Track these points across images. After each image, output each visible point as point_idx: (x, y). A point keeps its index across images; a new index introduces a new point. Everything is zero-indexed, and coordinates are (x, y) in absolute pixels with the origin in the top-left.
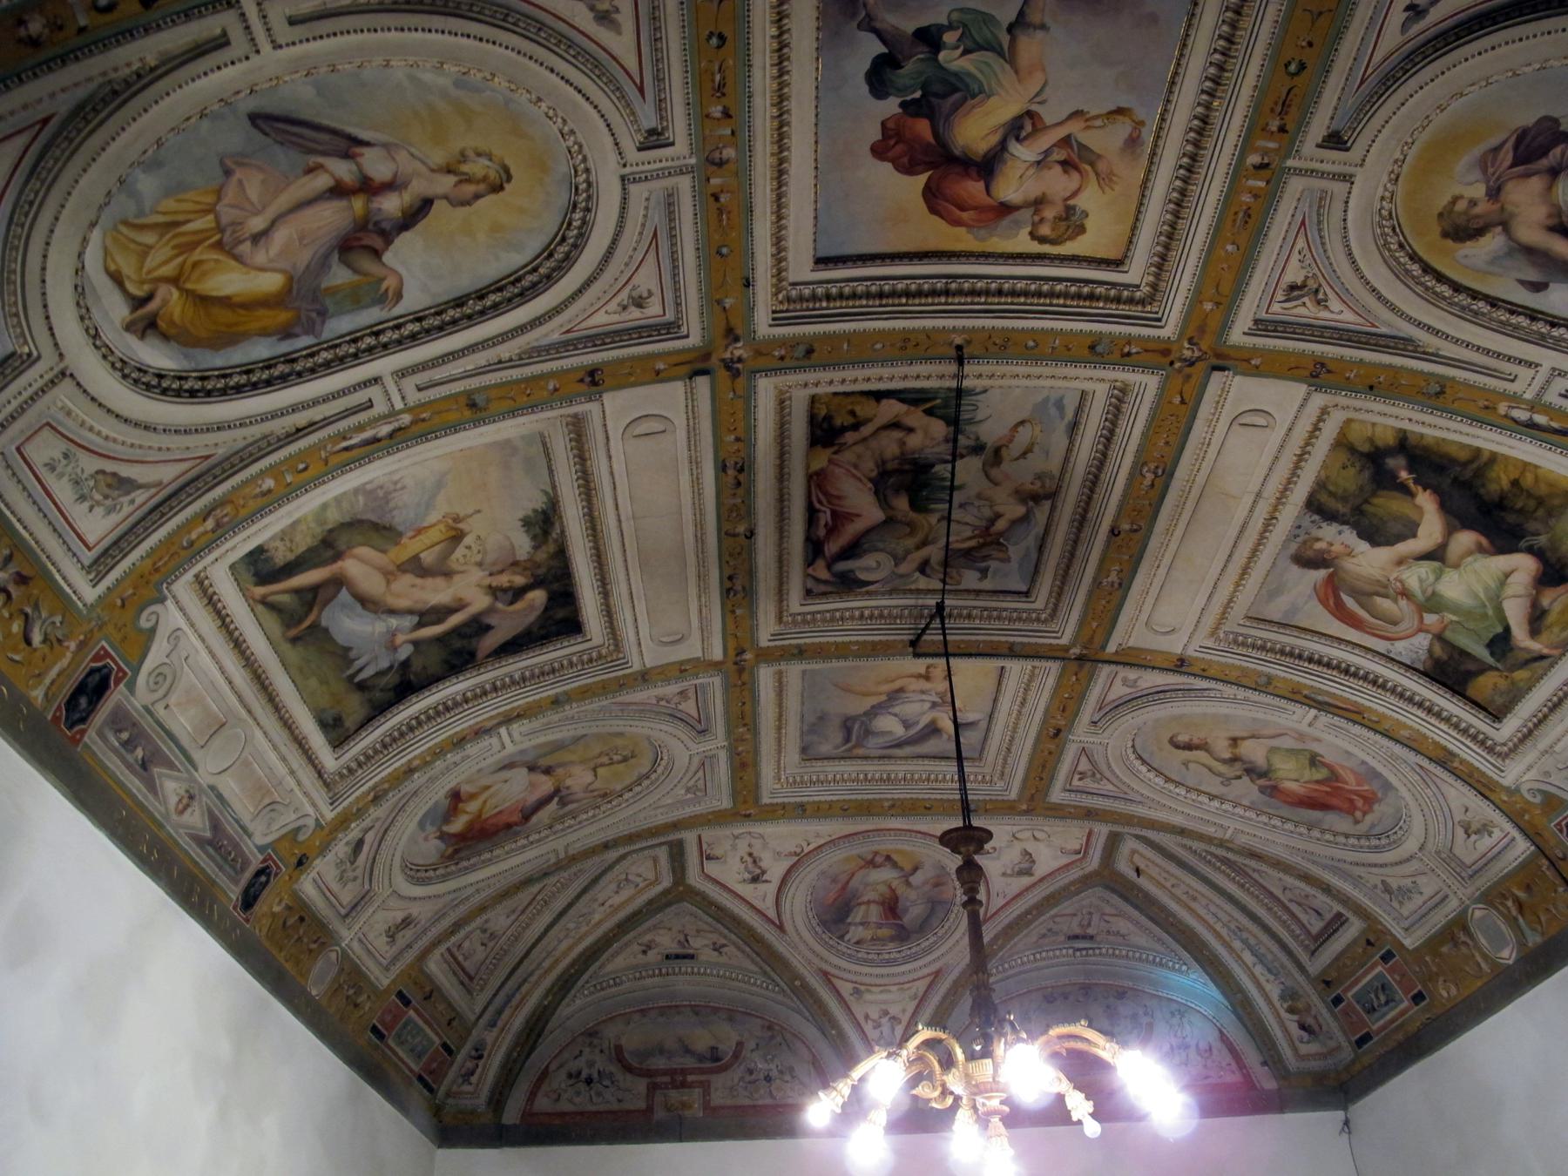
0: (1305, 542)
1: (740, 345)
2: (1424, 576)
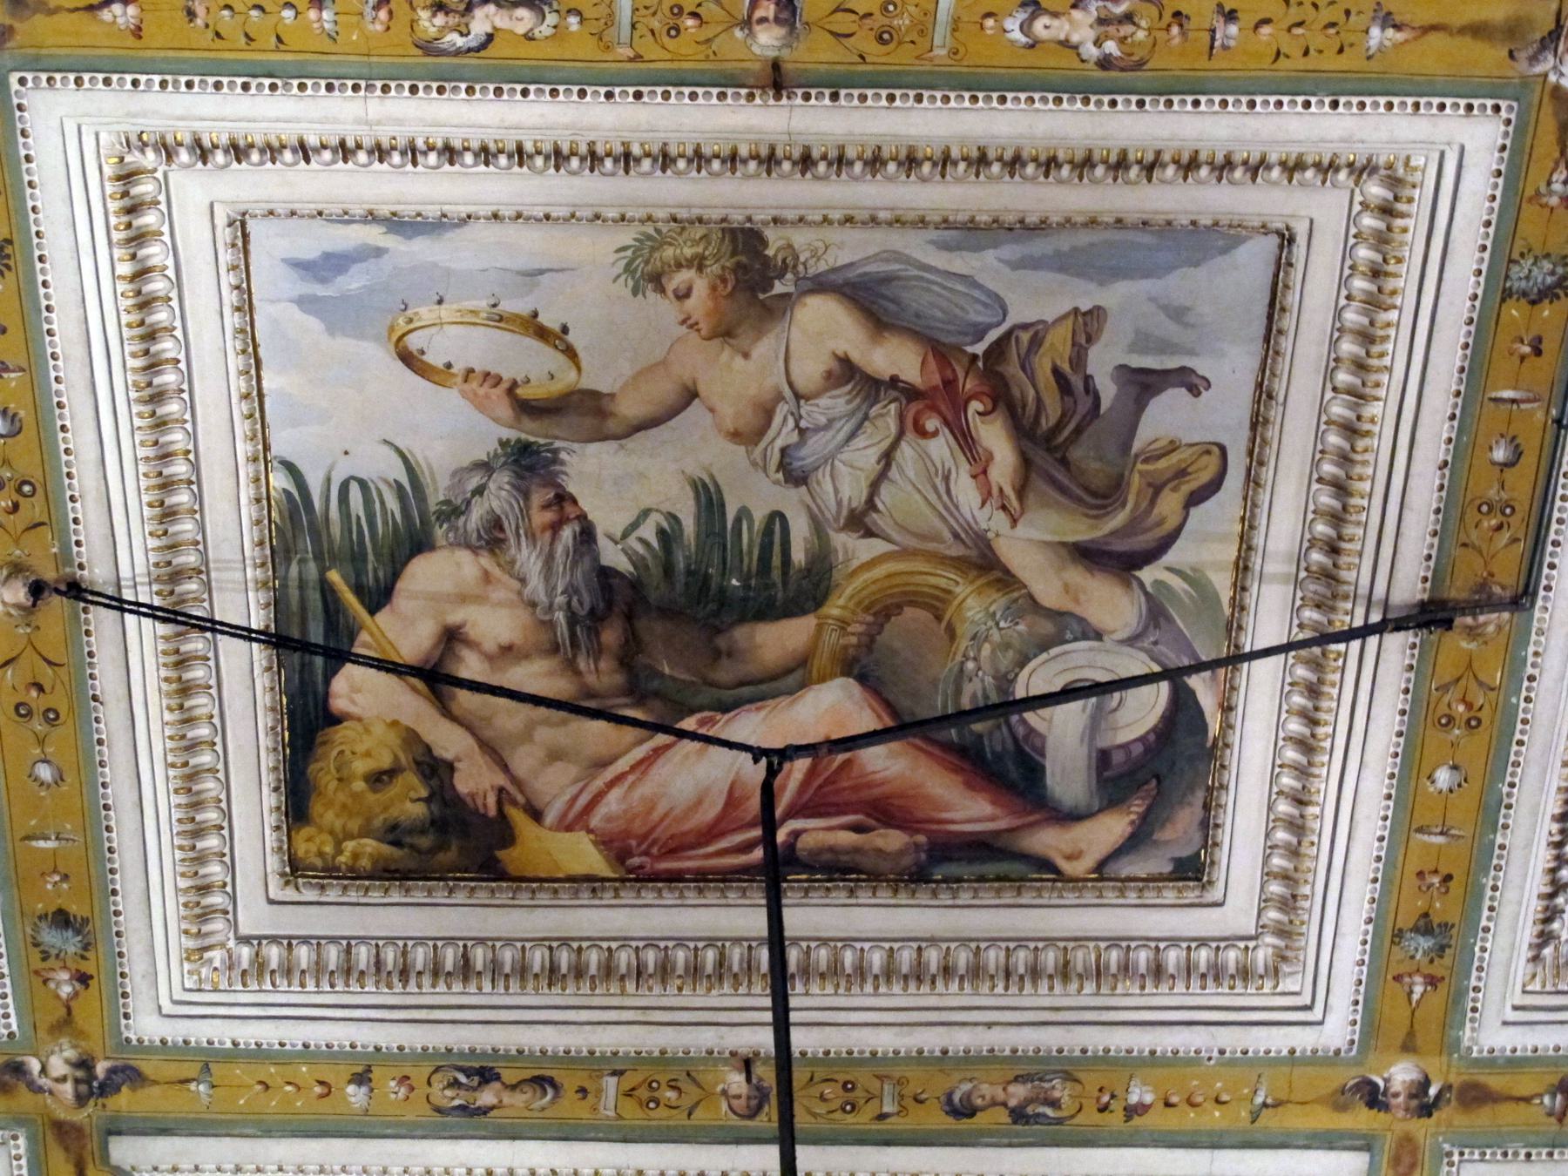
1: (34, 1065)
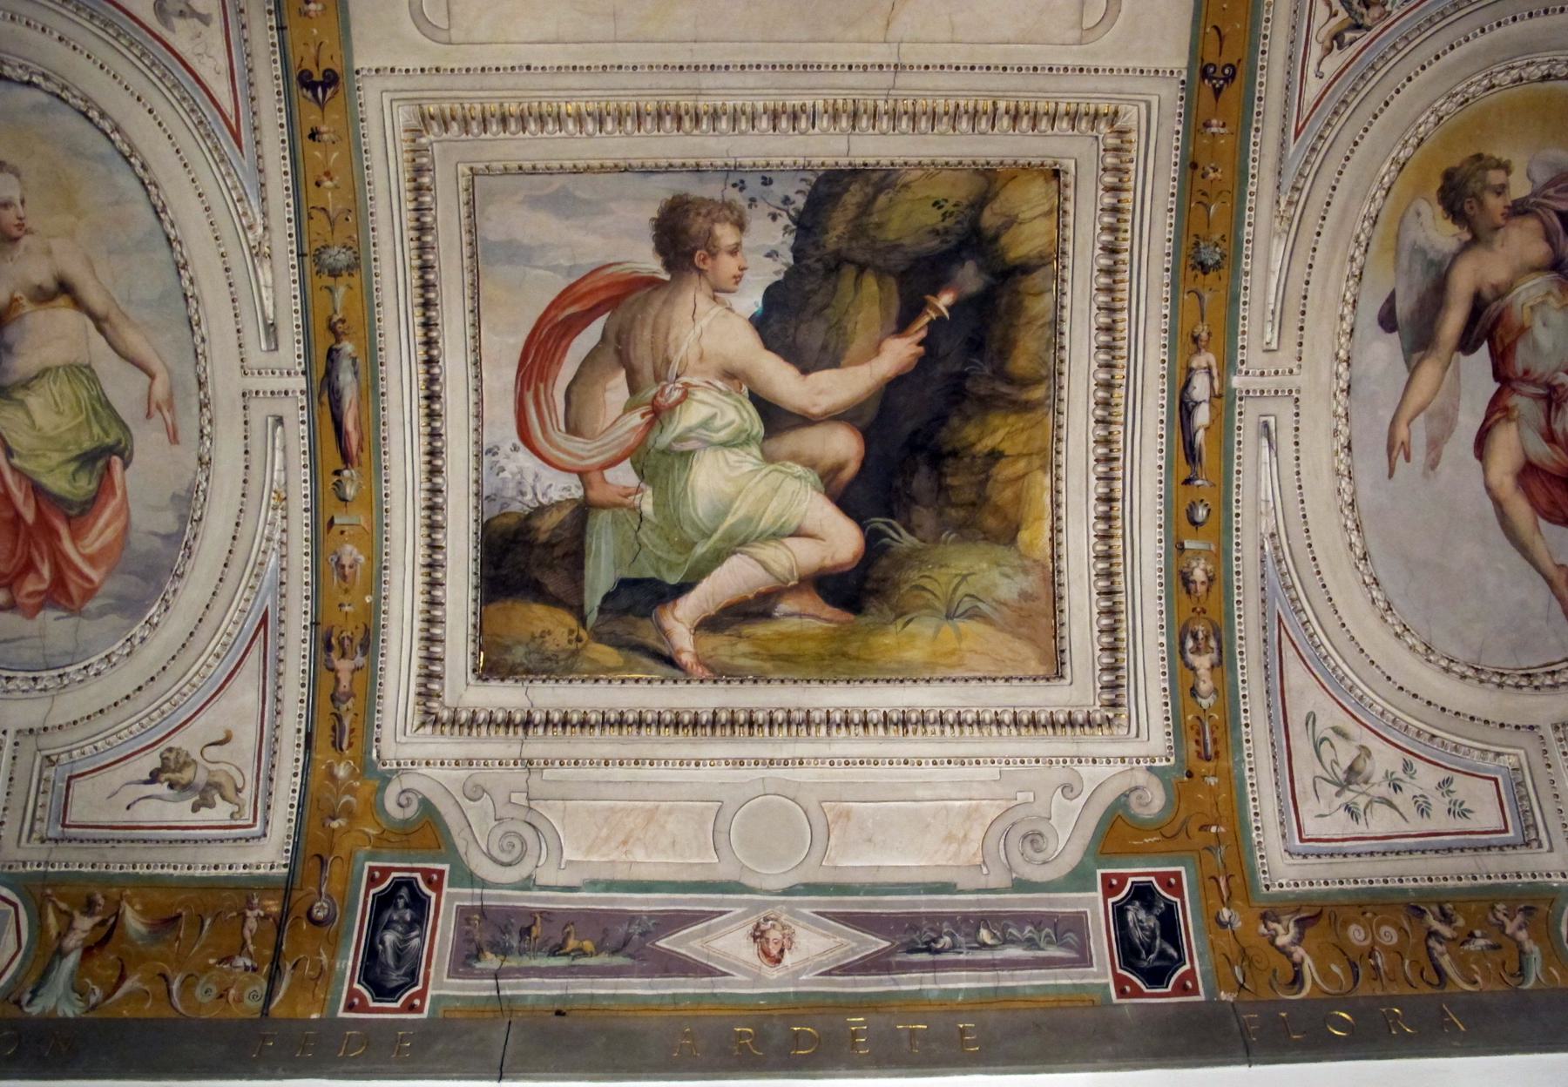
0: (729, 205)
2: (718, 423)
